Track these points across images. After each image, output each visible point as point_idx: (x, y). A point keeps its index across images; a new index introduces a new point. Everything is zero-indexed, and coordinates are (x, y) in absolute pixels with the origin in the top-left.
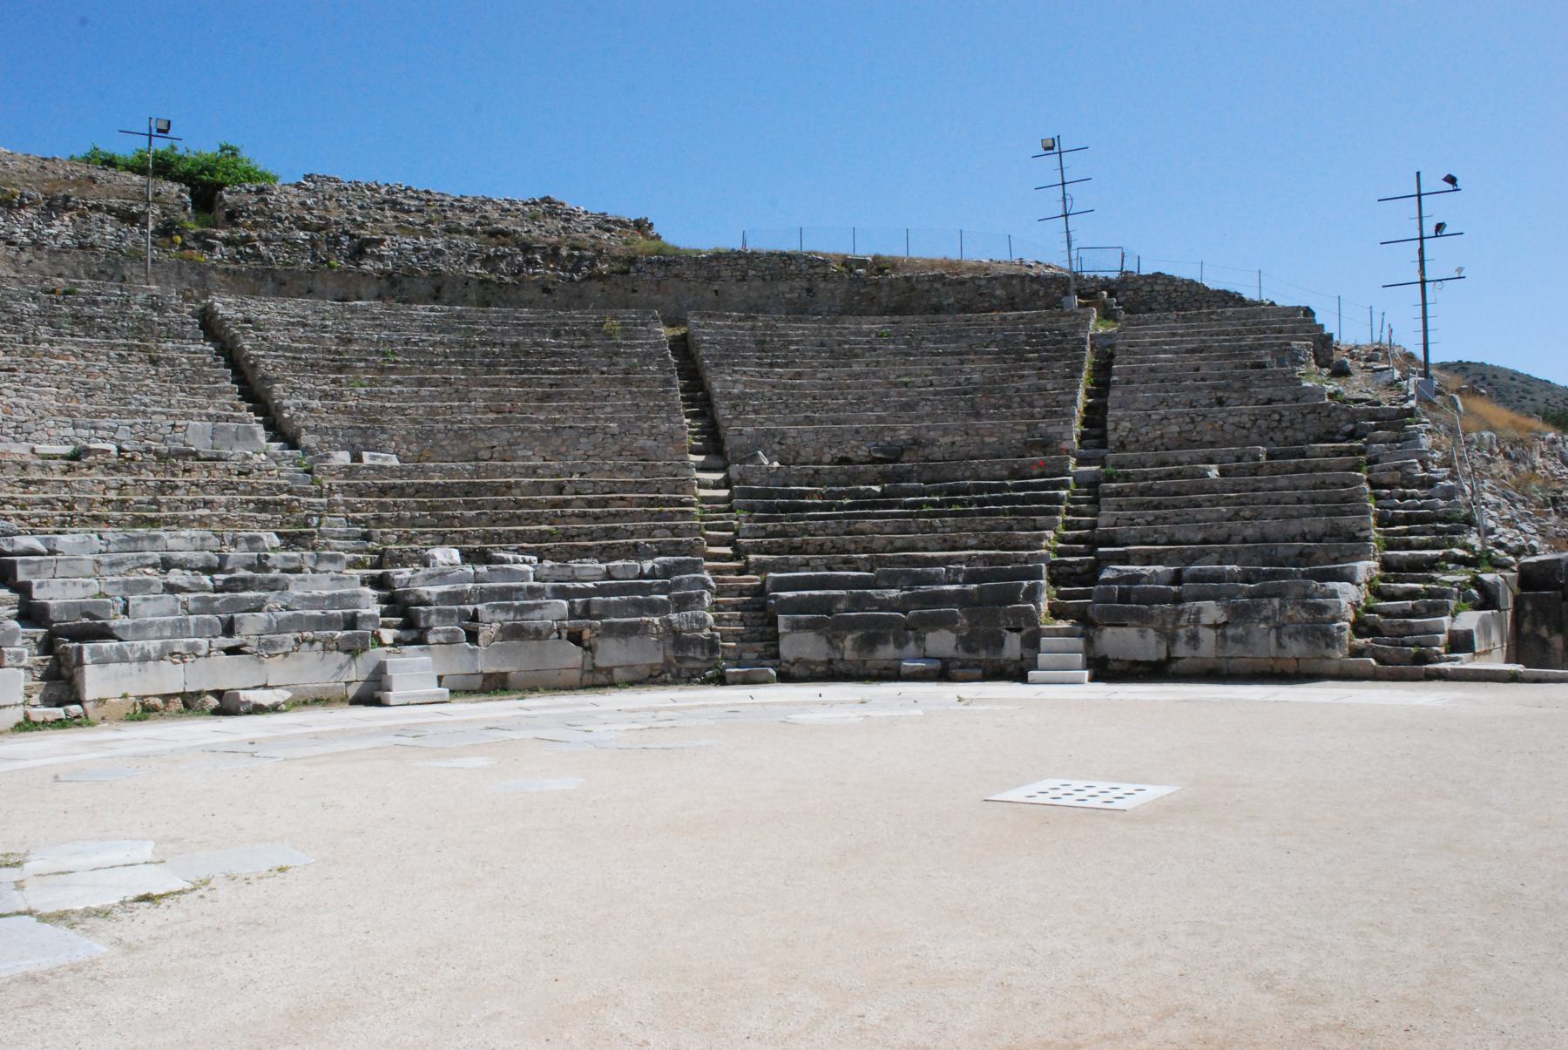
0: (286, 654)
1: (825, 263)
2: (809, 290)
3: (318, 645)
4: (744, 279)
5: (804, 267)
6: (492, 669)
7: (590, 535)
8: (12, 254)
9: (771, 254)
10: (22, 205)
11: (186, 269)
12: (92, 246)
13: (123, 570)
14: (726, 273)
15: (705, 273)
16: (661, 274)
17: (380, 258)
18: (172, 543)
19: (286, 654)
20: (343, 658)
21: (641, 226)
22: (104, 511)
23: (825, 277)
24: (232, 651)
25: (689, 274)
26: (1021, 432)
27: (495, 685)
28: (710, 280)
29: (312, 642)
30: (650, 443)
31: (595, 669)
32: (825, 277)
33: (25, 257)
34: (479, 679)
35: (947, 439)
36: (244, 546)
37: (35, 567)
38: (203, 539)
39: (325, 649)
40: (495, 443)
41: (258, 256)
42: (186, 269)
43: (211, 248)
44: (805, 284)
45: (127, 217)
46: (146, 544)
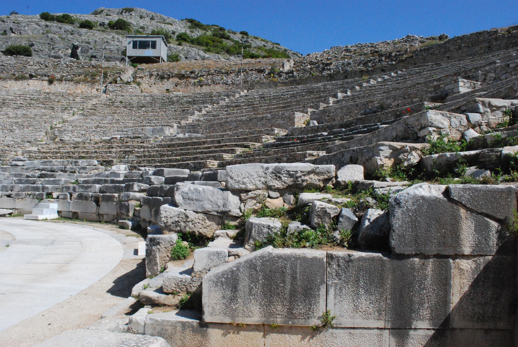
0: (22, 198)
1: (496, 32)
2: (489, 47)
3: (31, 196)
4: (460, 49)
5: (486, 36)
6: (74, 210)
7: (176, 160)
8: (227, 87)
9: (471, 35)
10: (231, 73)
11: (271, 84)
12: (248, 81)
13: (29, 171)
14: (452, 48)
15: (443, 50)
16: (425, 54)
17: (330, 70)
18: (55, 163)
19: (22, 198)
20: (37, 201)
22: (83, 155)
23: (496, 39)
24: (9, 196)
25: (437, 52)
26: (431, 92)
27: (74, 217)
28: (445, 52)
29: (30, 195)
30: (281, 122)
31: (99, 215)
32: (496, 39)
33: (230, 87)
34: (71, 214)
35: (396, 103)
36: (73, 164)
37: (4, 169)
38: (63, 162)
39: (33, 198)
40: (231, 127)
41: (293, 76)
42: (271, 84)
43: (280, 76)
44: (486, 45)
45: (260, 71)
46: (48, 163)
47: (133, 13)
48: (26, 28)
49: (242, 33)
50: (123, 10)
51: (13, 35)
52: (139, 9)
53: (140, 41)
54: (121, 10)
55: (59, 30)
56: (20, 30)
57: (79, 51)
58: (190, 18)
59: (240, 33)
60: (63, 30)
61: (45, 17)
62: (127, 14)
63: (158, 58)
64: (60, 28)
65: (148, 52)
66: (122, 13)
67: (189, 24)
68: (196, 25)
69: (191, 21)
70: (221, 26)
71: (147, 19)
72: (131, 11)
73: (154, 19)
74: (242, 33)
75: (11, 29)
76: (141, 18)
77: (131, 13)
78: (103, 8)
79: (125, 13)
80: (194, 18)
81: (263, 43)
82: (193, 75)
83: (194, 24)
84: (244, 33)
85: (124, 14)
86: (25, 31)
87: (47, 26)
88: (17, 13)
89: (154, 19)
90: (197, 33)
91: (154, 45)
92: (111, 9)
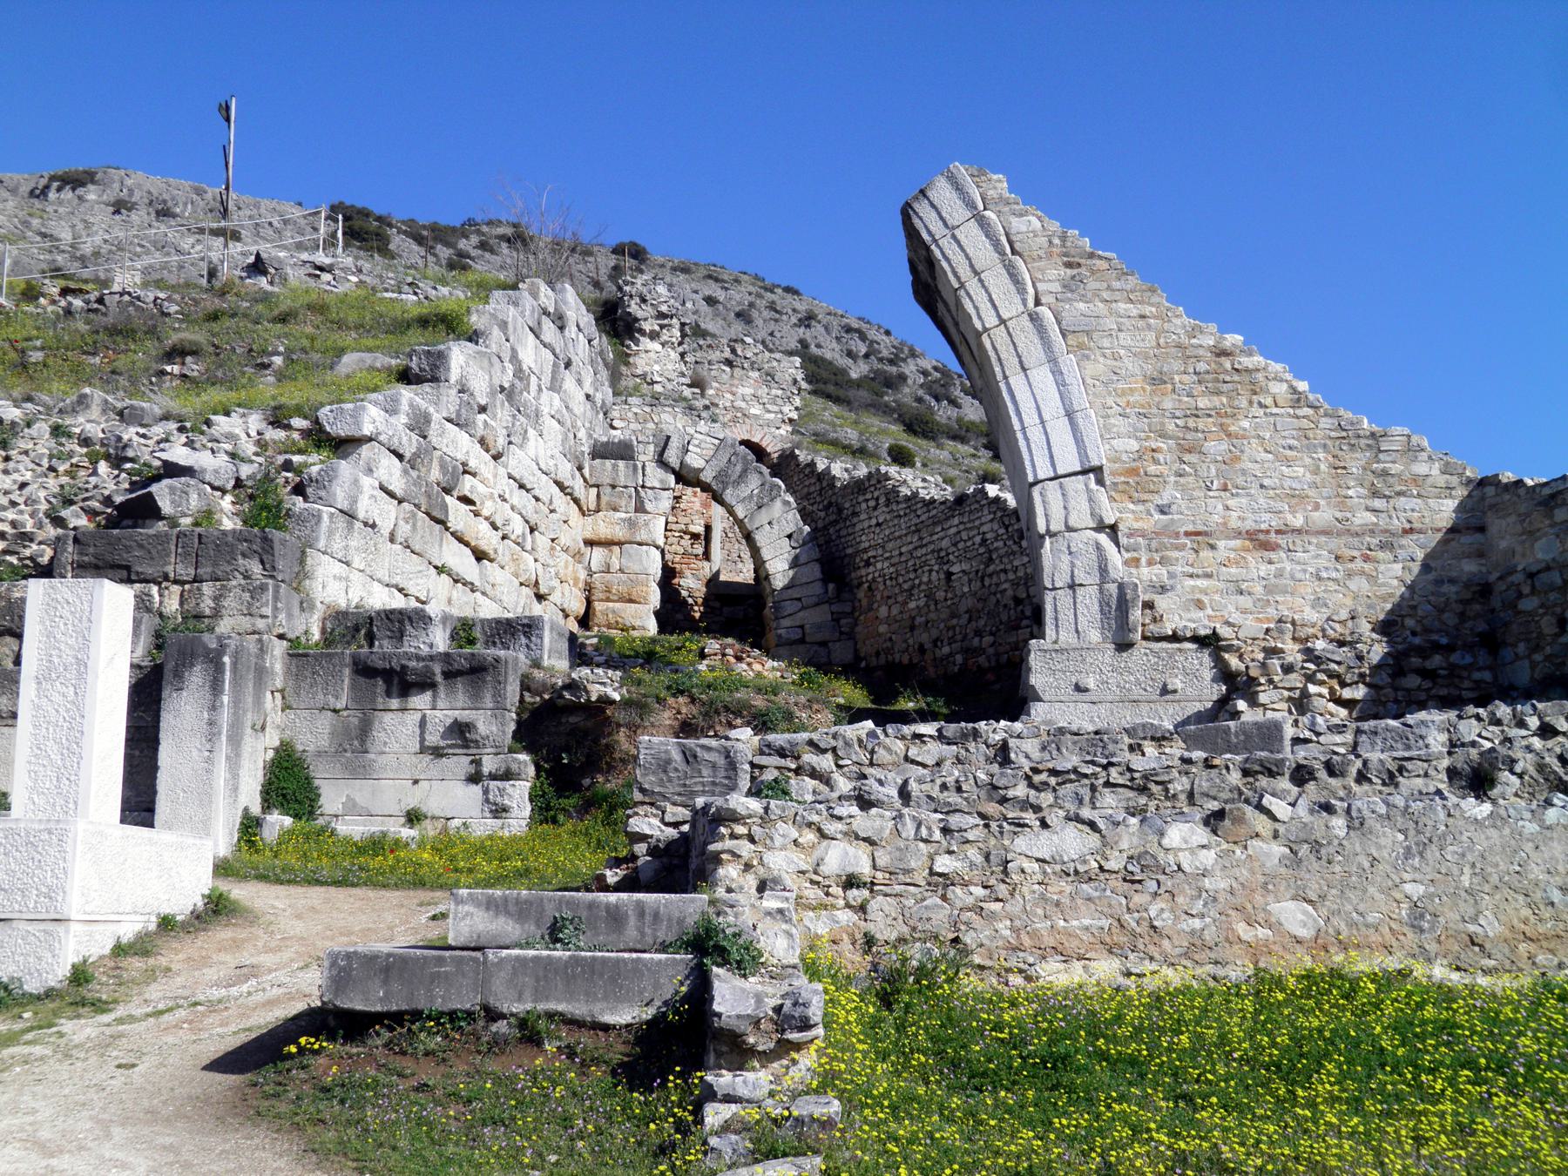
47: (91, 194)
49: (618, 250)
50: (52, 178)
54: (43, 182)
59: (614, 251)
62: (67, 194)
72: (83, 184)
73: (174, 216)
76: (117, 212)
79: (59, 190)
85: (52, 195)
89: (174, 216)
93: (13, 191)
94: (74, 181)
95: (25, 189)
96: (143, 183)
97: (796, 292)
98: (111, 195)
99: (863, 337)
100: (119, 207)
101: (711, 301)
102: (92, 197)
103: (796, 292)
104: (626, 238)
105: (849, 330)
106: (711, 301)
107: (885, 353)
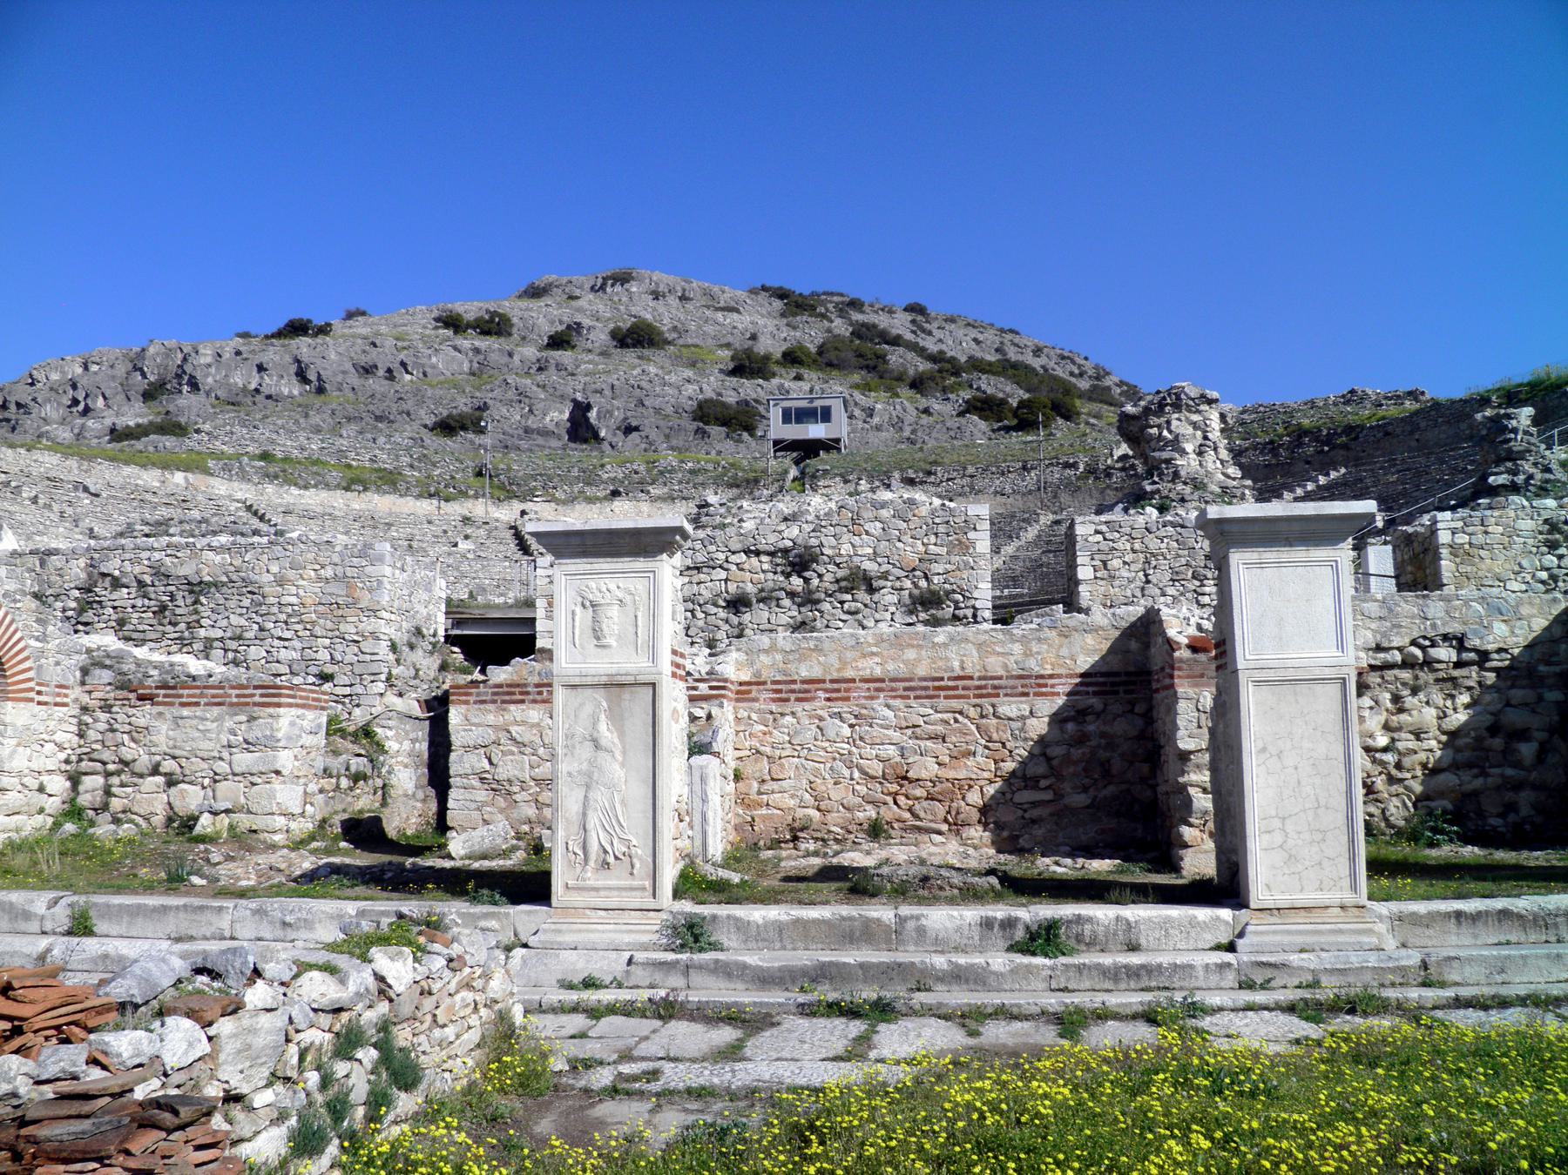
14: (1423, 424)
21: (1413, 395)
25: (1398, 431)
28: (1412, 433)
41: (1136, 475)
43: (1109, 475)
47: (634, 288)
48: (434, 359)
49: (910, 309)
51: (408, 377)
52: (645, 273)
53: (797, 409)
54: (600, 281)
55: (506, 359)
56: (423, 366)
57: (593, 415)
58: (776, 285)
59: (906, 310)
60: (516, 358)
61: (452, 323)
62: (618, 288)
63: (837, 441)
64: (510, 355)
65: (816, 431)
66: (603, 288)
67: (778, 304)
68: (798, 306)
69: (782, 294)
70: (853, 295)
71: (673, 301)
74: (910, 309)
75: (403, 364)
77: (627, 286)
78: (552, 278)
80: (787, 286)
81: (974, 333)
82: (932, 479)
83: (795, 304)
84: (915, 309)
85: (609, 289)
86: (434, 367)
87: (477, 351)
88: (363, 314)
90: (811, 335)
91: (826, 415)
92: (574, 279)
93: (581, 287)
94: (623, 279)
95: (587, 286)
96: (662, 279)
97: (1017, 333)
98: (645, 286)
99: (1073, 362)
100: (656, 296)
101: (975, 340)
102: (634, 289)
103: (1017, 333)
104: (911, 300)
105: (1063, 358)
106: (975, 340)
107: (1090, 373)
